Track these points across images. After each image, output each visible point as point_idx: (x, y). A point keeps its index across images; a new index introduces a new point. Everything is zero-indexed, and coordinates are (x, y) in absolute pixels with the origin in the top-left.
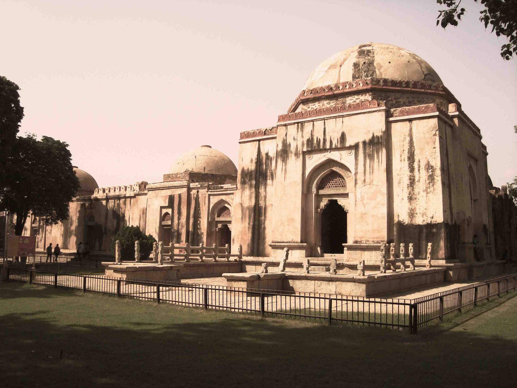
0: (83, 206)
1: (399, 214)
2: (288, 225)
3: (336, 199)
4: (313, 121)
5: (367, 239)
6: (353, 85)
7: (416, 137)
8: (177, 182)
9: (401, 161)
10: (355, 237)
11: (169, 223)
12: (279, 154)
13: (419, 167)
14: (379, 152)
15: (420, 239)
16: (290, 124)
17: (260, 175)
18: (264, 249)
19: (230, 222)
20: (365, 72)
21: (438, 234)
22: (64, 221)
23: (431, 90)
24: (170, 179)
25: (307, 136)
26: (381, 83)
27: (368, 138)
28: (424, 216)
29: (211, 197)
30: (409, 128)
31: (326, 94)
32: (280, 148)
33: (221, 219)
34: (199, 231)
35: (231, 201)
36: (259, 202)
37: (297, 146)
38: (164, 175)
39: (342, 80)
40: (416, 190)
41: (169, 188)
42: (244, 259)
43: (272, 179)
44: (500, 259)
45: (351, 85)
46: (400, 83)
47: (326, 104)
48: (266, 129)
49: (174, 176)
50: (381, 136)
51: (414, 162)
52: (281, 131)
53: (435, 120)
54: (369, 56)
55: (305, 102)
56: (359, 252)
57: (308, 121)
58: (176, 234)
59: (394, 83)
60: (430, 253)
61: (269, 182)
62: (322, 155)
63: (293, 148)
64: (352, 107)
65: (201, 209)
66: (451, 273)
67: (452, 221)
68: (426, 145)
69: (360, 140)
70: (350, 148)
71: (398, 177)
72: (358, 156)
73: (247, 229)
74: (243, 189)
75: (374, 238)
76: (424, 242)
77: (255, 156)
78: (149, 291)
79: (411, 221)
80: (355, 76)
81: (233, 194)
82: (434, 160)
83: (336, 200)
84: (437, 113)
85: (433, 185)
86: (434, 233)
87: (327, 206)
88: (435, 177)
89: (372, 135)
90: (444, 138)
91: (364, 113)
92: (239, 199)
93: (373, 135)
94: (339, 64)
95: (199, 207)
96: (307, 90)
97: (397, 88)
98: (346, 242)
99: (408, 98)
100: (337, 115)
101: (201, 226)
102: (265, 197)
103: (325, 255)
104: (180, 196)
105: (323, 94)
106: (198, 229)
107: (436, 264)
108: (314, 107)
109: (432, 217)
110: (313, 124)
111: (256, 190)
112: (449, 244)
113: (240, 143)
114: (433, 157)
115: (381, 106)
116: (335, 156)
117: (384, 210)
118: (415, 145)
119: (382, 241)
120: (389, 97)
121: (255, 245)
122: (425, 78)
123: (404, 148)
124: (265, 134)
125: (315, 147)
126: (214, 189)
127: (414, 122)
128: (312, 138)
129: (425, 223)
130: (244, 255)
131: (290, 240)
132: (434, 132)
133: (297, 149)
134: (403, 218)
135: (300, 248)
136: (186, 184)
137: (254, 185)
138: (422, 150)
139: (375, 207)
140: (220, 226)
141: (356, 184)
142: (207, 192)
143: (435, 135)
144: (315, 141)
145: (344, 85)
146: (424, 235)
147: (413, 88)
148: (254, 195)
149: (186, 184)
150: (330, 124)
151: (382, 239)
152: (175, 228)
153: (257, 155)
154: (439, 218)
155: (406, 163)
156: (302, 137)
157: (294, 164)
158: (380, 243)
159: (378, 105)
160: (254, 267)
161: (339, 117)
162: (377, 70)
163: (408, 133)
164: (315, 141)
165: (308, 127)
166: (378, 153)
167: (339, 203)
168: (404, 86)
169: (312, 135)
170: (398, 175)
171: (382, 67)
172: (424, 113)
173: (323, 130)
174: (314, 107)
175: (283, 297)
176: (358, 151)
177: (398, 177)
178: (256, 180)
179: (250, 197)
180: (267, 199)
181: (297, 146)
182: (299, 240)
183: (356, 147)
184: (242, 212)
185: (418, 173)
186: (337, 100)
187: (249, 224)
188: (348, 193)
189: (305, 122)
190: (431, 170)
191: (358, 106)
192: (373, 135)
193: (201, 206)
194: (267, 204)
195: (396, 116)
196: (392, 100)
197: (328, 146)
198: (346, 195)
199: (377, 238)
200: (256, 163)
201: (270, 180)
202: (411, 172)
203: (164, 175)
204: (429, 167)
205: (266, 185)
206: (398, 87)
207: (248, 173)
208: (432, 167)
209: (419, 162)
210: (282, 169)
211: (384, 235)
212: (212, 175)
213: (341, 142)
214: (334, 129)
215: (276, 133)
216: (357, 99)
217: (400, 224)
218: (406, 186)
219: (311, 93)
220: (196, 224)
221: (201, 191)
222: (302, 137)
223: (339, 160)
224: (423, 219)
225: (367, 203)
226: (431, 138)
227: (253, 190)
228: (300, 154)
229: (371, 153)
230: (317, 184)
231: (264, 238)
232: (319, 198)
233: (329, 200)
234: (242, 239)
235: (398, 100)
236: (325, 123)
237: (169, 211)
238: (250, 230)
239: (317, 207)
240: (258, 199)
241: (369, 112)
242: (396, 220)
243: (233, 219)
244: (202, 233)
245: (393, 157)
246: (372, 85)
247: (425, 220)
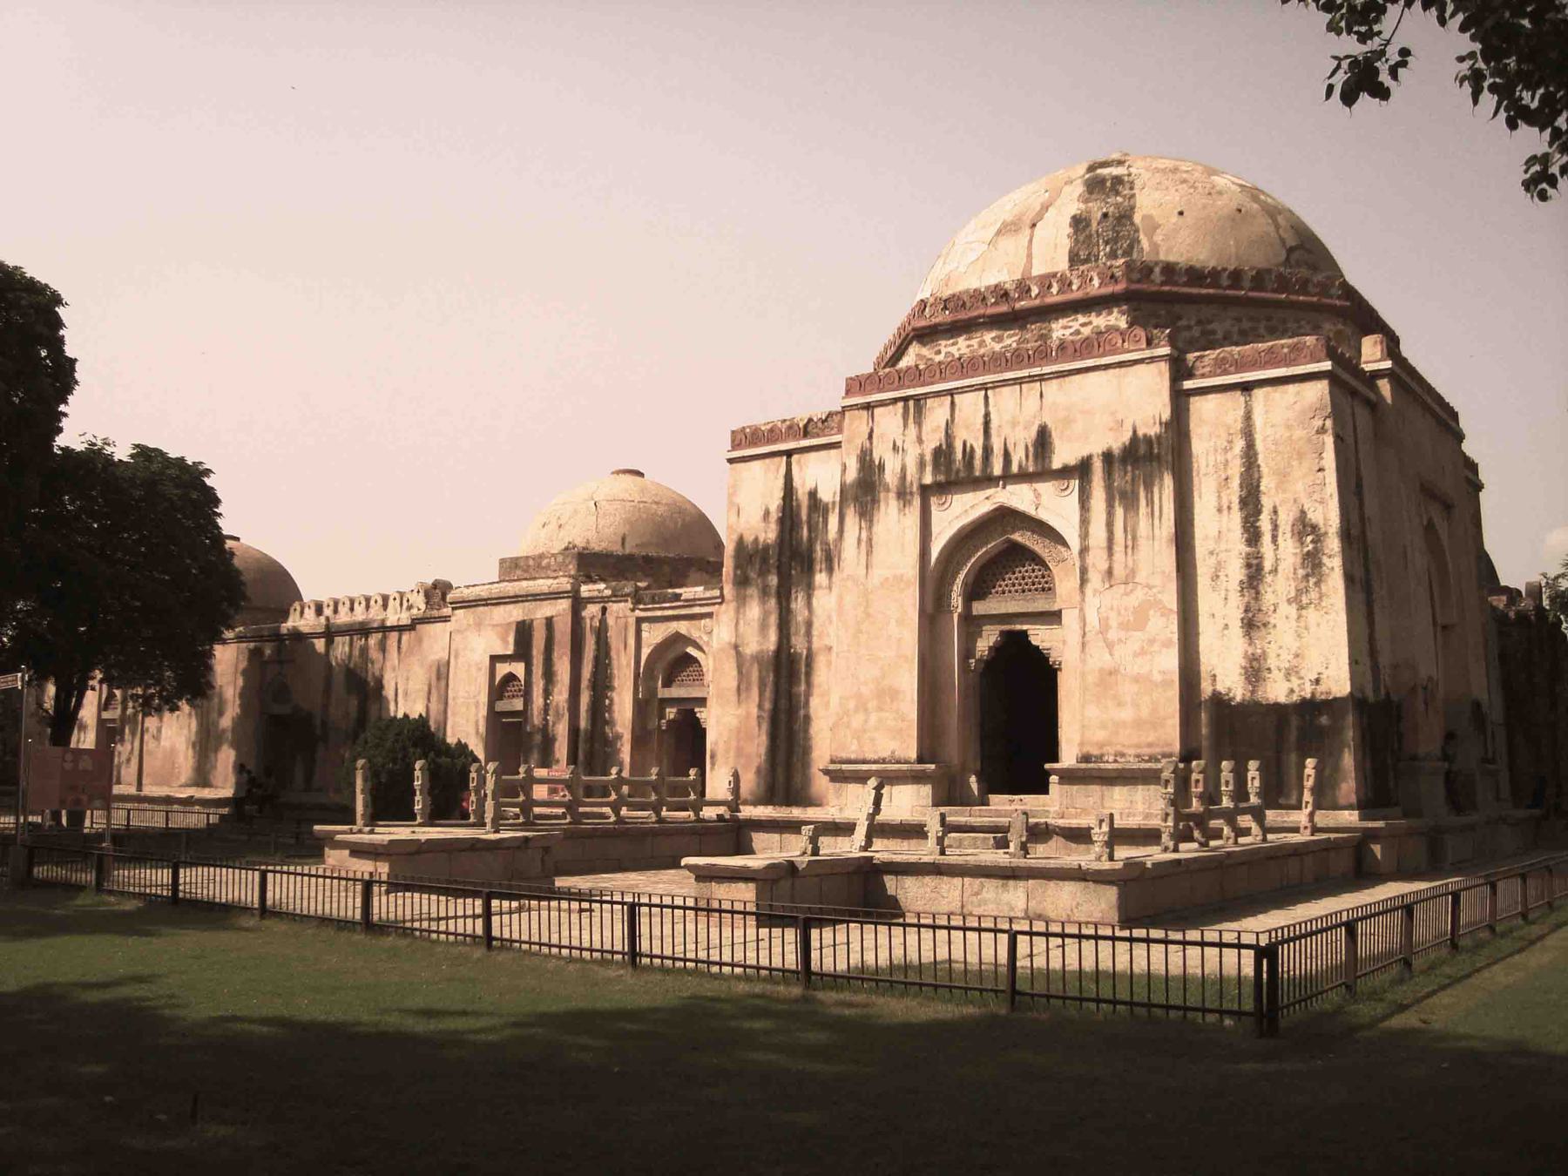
0: (255, 654)
1: (1216, 672)
2: (880, 709)
3: (1025, 627)
4: (951, 393)
5: (1119, 748)
6: (1070, 284)
7: (1264, 440)
8: (541, 582)
9: (1220, 510)
10: (1082, 744)
11: (518, 705)
12: (850, 494)
13: (1275, 527)
14: (1152, 485)
15: (1279, 752)
16: (882, 403)
17: (792, 558)
18: (807, 780)
19: (702, 702)
20: (1107, 243)
21: (1336, 730)
22: (198, 702)
23: (1307, 294)
24: (519, 572)
25: (933, 439)
26: (1157, 275)
27: (1117, 441)
28: (1293, 679)
29: (645, 626)
30: (1241, 412)
31: (990, 311)
32: (852, 475)
33: (676, 692)
34: (607, 729)
35: (705, 638)
36: (789, 640)
37: (903, 469)
38: (502, 561)
39: (1036, 272)
40: (1268, 598)
41: (516, 599)
42: (747, 812)
43: (830, 570)
44: (1529, 807)
45: (1066, 284)
46: (1215, 274)
47: (990, 342)
48: (810, 420)
49: (531, 562)
50: (1159, 437)
51: (1259, 512)
52: (856, 423)
53: (1322, 386)
54: (1118, 193)
55: (926, 335)
56: (1095, 789)
57: (938, 394)
58: (538, 738)
59: (1195, 275)
60: (1312, 790)
61: (820, 578)
62: (982, 494)
63: (890, 477)
64: (1070, 350)
65: (615, 663)
66: (1377, 849)
67: (1376, 690)
68: (1295, 463)
69: (1095, 446)
70: (1065, 473)
73: (754, 723)
74: (741, 601)
75: (1138, 746)
76: (1293, 757)
77: (775, 503)
78: (460, 913)
79: (1253, 692)
80: (1077, 255)
81: (709, 615)
82: (1320, 508)
83: (1024, 634)
84: (1327, 365)
85: (1317, 584)
86: (1321, 732)
87: (996, 650)
88: (1325, 560)
89: (1130, 434)
90: (1350, 440)
91: (1107, 367)
92: (727, 632)
93: (1135, 432)
94: (1028, 222)
95: (608, 654)
96: (932, 300)
97: (1204, 291)
98: (1056, 759)
99: (1239, 320)
100: (1025, 373)
101: (616, 715)
102: (809, 624)
103: (993, 798)
104: (549, 622)
105: (981, 311)
106: (607, 722)
107: (1332, 824)
108: (953, 350)
109: (1317, 681)
110: (953, 403)
111: (780, 603)
112: (1368, 765)
113: (731, 461)
114: (1316, 496)
115: (1157, 346)
116: (1019, 497)
117: (1170, 661)
118: (1261, 460)
119: (1165, 756)
120: (1180, 318)
121: (780, 770)
122: (1287, 259)
123: (1230, 472)
124: (806, 434)
125: (958, 471)
126: (654, 602)
127: (1259, 393)
128: (950, 445)
129: (1295, 698)
130: (746, 803)
131: (886, 754)
132: (1318, 423)
133: (903, 477)
134: (1228, 684)
135: (917, 778)
136: (569, 587)
137: (773, 591)
138: (1283, 476)
139: (1142, 652)
140: (671, 713)
141: (1084, 581)
142: (633, 610)
143: (1322, 430)
144: (959, 455)
145: (1046, 281)
146: (1293, 736)
147: (1252, 289)
148: (773, 620)
149: (569, 587)
150: (1005, 402)
151: (1166, 750)
152: (537, 720)
153: (784, 498)
154: (1338, 682)
155: (1236, 518)
156: (920, 440)
157: (896, 525)
158: (1158, 761)
159: (1149, 343)
160: (776, 837)
161: (1032, 379)
162: (1142, 237)
163: (1239, 425)
164: (959, 455)
165: (937, 413)
166: (1149, 488)
167: (1034, 641)
168: (1225, 282)
169: (949, 436)
170: (1211, 553)
171: (1156, 227)
172: (1287, 366)
173: (980, 420)
174: (953, 350)
175: (869, 928)
176: (1090, 482)
177: (1212, 561)
178: (780, 574)
179: (763, 627)
180: (815, 632)
181: (903, 469)
182: (913, 755)
183: (1081, 470)
184: (740, 672)
185: (1272, 547)
186: (1023, 328)
187: (760, 707)
189: (926, 396)
190: (1310, 538)
191: (1084, 347)
192: (1135, 432)
193: (613, 654)
194: (816, 644)
195: (1203, 376)
196: (1189, 328)
197: (997, 470)
198: (1054, 617)
199: (1150, 745)
200: (781, 521)
201: (824, 574)
203: (502, 561)
204: (1305, 528)
205: (810, 588)
206: (1208, 287)
207: (757, 551)
208: (1314, 528)
209: (1275, 512)
210: (859, 540)
211: (1170, 735)
212: (647, 559)
214: (1014, 414)
215: (840, 431)
216: (1083, 325)
217: (1220, 702)
218: (1234, 586)
219: (945, 308)
220: (600, 709)
221: (616, 608)
222: (920, 440)
223: (1032, 512)
224: (1287, 685)
225: (1120, 640)
226: (1309, 440)
227: (772, 603)
228: (911, 493)
229: (1129, 488)
230: (965, 584)
231: (807, 751)
232: (972, 624)
233: (1002, 633)
234: (740, 752)
235: (1210, 327)
236: (986, 397)
237: (518, 669)
238: (765, 726)
239: (967, 652)
240: (788, 629)
241: (1121, 365)
242: (1206, 689)
243: (711, 693)
244: (619, 737)
245: (1196, 499)
246: (1130, 281)
247: (1297, 689)
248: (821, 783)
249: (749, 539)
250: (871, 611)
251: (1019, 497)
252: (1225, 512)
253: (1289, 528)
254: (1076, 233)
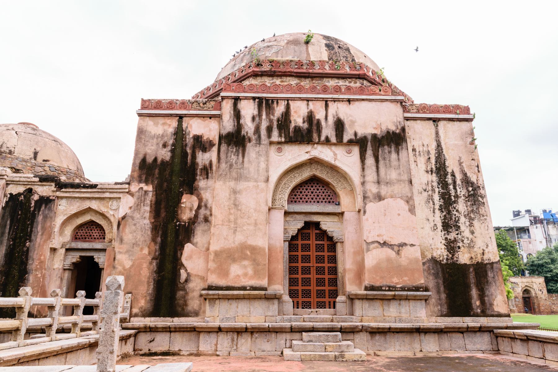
4: (288, 100)
9: (427, 172)
31: (295, 71)
51: (447, 175)
71: (425, 194)
72: (365, 159)
88: (480, 199)
109: (483, 254)
116: (325, 153)
127: (441, 124)
129: (474, 262)
134: (439, 252)
145: (322, 63)
167: (323, 227)
170: (425, 190)
176: (366, 150)
177: (425, 194)
188: (342, 214)
202: (443, 189)
208: (472, 184)
213: (337, 136)
218: (437, 207)
223: (333, 162)
233: (306, 223)
236: (308, 105)
248: (194, 304)
249: (150, 160)
250: (237, 203)
251: (325, 153)
252: (430, 173)
253: (460, 183)
254: (329, 49)
